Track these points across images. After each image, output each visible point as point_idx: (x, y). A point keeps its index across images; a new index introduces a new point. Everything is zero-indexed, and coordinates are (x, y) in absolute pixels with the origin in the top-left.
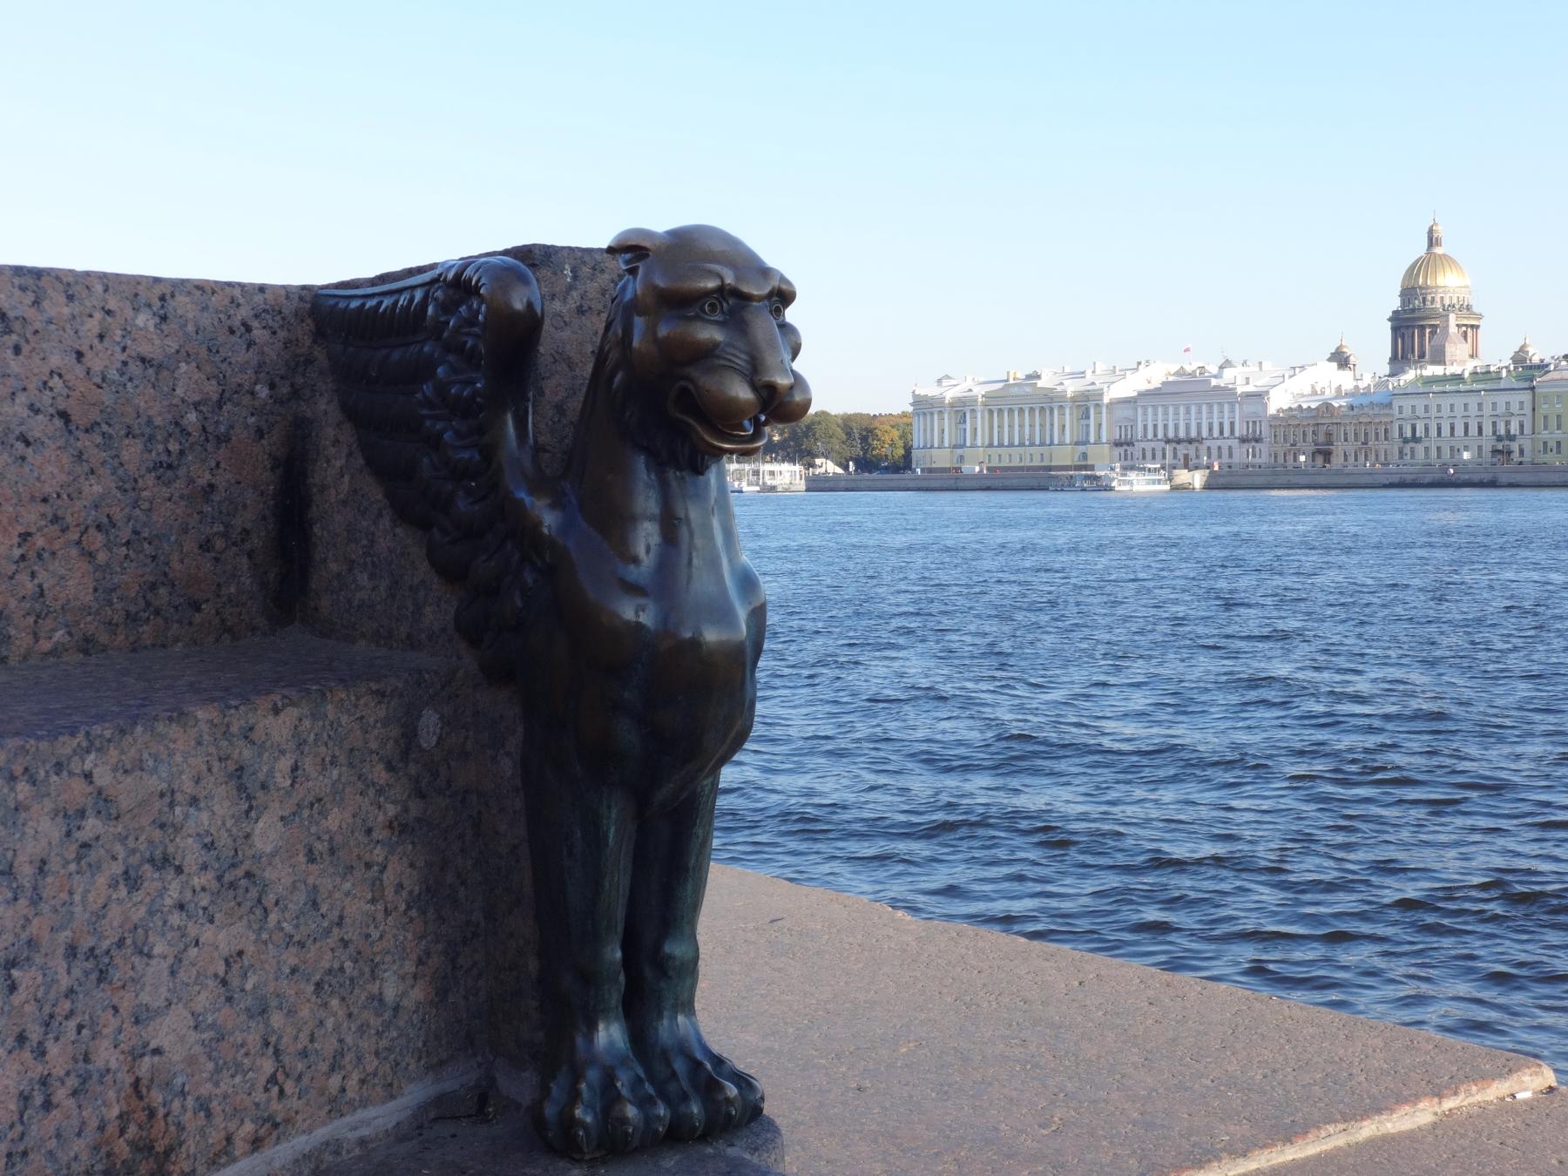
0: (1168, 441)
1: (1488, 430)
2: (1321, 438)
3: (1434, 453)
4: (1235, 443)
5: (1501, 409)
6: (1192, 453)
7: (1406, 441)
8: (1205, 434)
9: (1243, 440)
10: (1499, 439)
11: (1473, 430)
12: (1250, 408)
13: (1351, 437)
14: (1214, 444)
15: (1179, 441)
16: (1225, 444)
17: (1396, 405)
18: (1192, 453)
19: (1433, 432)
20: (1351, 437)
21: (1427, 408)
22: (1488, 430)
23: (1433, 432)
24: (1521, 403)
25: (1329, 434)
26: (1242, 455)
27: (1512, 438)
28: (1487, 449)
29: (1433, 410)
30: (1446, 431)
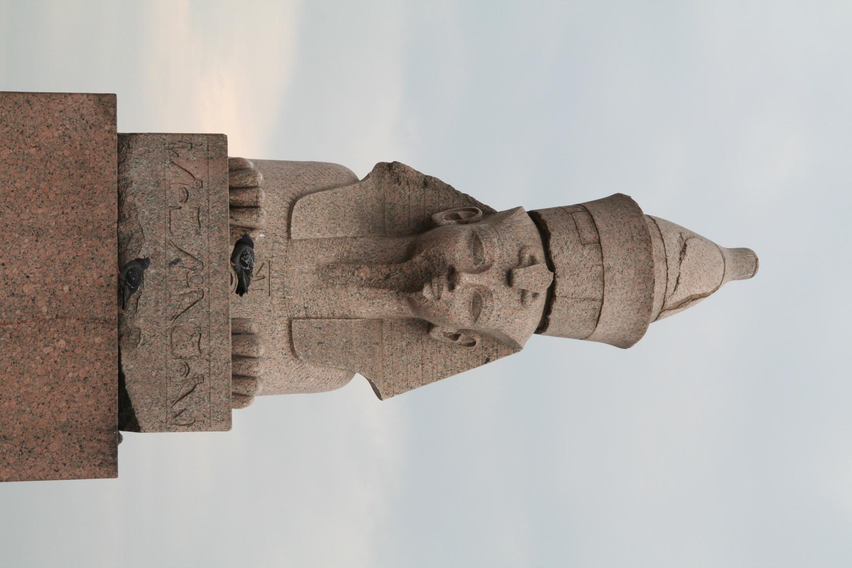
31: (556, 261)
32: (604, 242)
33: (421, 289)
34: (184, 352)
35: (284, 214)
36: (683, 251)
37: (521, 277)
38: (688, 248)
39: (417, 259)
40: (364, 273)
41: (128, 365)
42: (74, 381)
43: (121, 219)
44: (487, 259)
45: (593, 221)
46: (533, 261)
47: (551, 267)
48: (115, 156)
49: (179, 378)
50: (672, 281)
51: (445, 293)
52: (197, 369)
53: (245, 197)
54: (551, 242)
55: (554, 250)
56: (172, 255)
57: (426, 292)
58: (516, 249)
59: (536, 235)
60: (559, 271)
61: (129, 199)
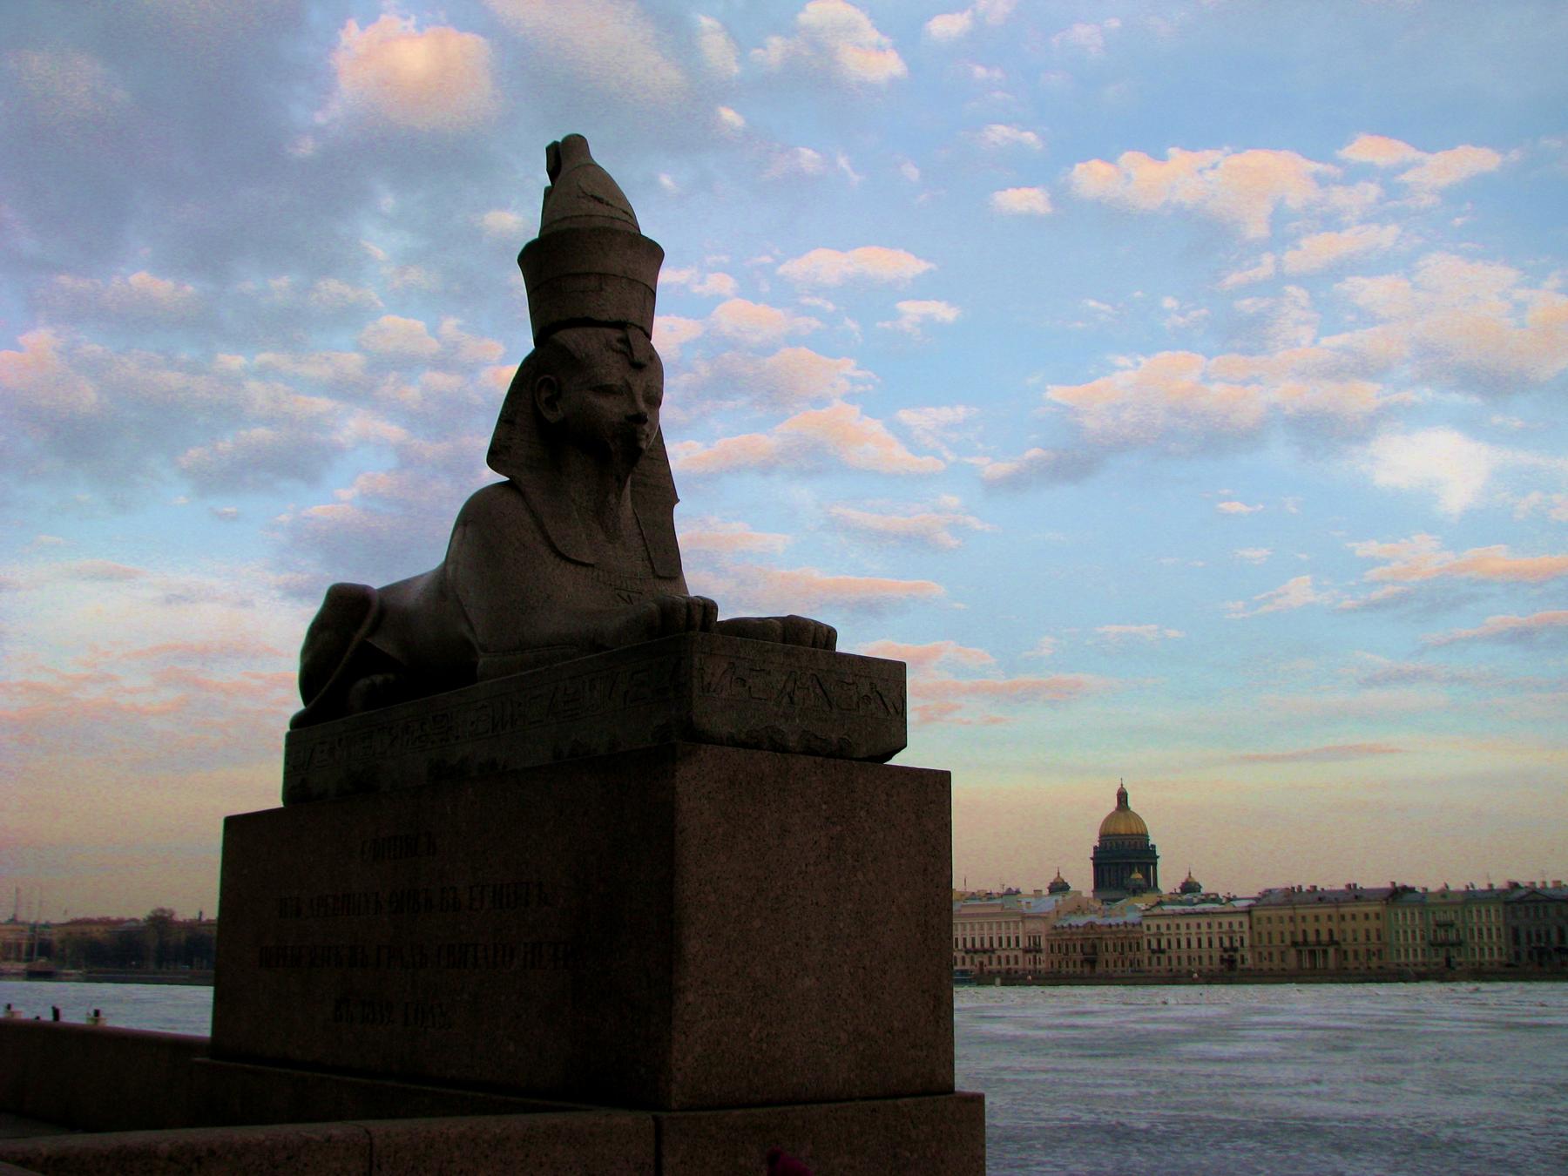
0: (967, 952)
1: (1216, 943)
2: (1087, 949)
3: (1174, 962)
4: (1020, 954)
5: (1225, 927)
6: (986, 962)
7: (1154, 952)
8: (996, 945)
9: (1026, 951)
10: (1225, 950)
11: (1205, 944)
12: (1031, 926)
13: (1111, 948)
14: (1003, 954)
15: (976, 952)
16: (1012, 954)
17: (1145, 923)
18: (986, 962)
19: (1174, 945)
20: (1111, 948)
21: (1168, 927)
22: (1216, 943)
23: (1174, 945)
24: (1241, 924)
25: (1094, 946)
26: (1024, 963)
27: (1235, 950)
28: (1216, 960)
29: (1173, 927)
30: (1184, 944)
31: (615, 318)
32: (599, 269)
33: (641, 450)
34: (855, 699)
35: (572, 567)
36: (600, 200)
37: (639, 356)
38: (597, 194)
39: (612, 447)
40: (612, 499)
41: (863, 751)
42: (888, 805)
43: (758, 746)
44: (620, 383)
45: (577, 275)
46: (625, 341)
47: (621, 325)
48: (726, 749)
49: (873, 706)
50: (626, 217)
51: (646, 428)
52: (865, 690)
53: (698, 617)
54: (598, 317)
55: (605, 318)
56: (786, 699)
57: (644, 445)
58: (611, 353)
59: (590, 331)
60: (623, 319)
61: (743, 736)
